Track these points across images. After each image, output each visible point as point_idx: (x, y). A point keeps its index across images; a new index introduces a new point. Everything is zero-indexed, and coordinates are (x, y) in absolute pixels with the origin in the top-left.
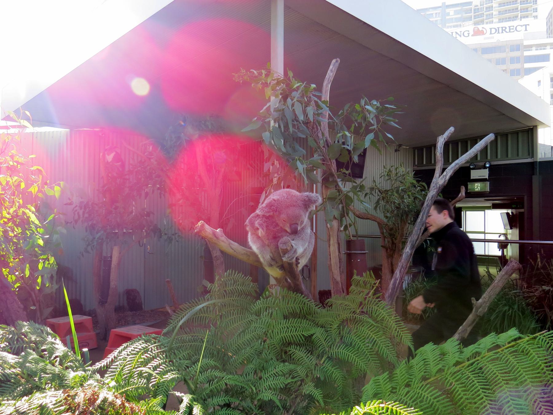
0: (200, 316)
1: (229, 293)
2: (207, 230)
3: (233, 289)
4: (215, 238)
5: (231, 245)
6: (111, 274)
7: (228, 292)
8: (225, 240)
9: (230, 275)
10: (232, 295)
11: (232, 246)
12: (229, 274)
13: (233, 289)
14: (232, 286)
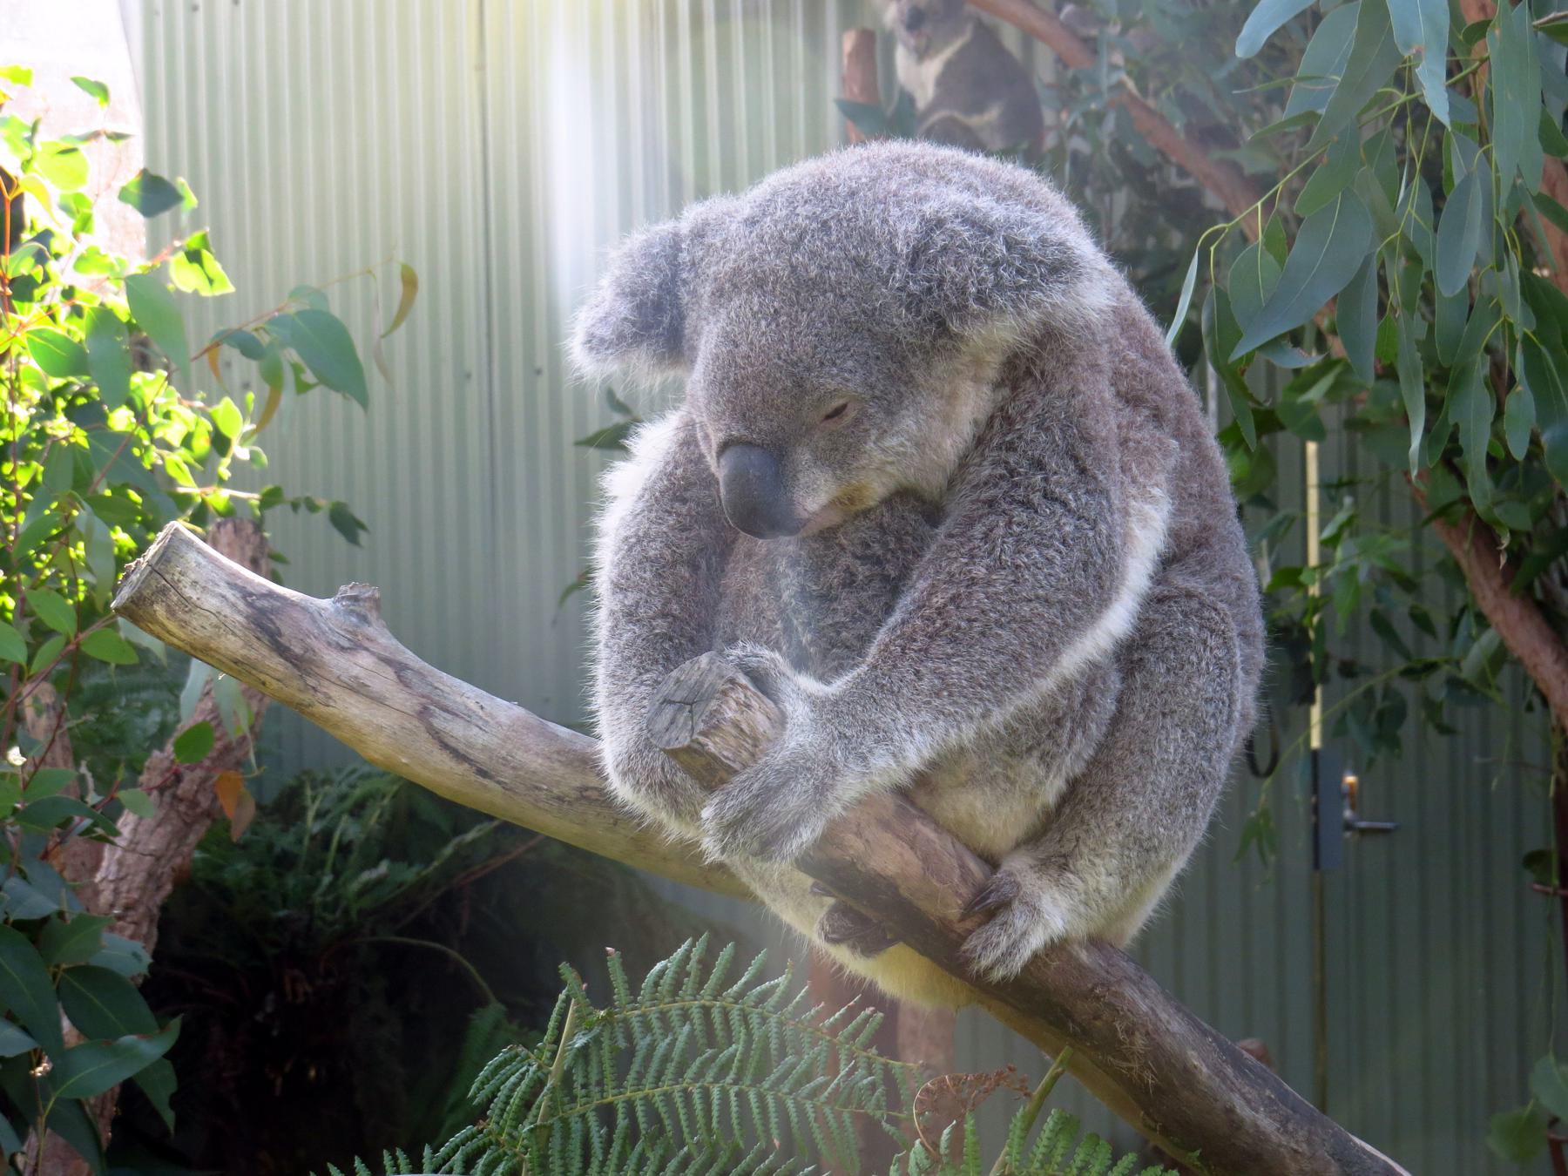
1: (633, 1135)
2: (189, 592)
3: (668, 1097)
4: (276, 663)
5: (441, 721)
7: (622, 1122)
8: (383, 681)
9: (689, 983)
11: (455, 730)
12: (681, 972)
14: (671, 1068)
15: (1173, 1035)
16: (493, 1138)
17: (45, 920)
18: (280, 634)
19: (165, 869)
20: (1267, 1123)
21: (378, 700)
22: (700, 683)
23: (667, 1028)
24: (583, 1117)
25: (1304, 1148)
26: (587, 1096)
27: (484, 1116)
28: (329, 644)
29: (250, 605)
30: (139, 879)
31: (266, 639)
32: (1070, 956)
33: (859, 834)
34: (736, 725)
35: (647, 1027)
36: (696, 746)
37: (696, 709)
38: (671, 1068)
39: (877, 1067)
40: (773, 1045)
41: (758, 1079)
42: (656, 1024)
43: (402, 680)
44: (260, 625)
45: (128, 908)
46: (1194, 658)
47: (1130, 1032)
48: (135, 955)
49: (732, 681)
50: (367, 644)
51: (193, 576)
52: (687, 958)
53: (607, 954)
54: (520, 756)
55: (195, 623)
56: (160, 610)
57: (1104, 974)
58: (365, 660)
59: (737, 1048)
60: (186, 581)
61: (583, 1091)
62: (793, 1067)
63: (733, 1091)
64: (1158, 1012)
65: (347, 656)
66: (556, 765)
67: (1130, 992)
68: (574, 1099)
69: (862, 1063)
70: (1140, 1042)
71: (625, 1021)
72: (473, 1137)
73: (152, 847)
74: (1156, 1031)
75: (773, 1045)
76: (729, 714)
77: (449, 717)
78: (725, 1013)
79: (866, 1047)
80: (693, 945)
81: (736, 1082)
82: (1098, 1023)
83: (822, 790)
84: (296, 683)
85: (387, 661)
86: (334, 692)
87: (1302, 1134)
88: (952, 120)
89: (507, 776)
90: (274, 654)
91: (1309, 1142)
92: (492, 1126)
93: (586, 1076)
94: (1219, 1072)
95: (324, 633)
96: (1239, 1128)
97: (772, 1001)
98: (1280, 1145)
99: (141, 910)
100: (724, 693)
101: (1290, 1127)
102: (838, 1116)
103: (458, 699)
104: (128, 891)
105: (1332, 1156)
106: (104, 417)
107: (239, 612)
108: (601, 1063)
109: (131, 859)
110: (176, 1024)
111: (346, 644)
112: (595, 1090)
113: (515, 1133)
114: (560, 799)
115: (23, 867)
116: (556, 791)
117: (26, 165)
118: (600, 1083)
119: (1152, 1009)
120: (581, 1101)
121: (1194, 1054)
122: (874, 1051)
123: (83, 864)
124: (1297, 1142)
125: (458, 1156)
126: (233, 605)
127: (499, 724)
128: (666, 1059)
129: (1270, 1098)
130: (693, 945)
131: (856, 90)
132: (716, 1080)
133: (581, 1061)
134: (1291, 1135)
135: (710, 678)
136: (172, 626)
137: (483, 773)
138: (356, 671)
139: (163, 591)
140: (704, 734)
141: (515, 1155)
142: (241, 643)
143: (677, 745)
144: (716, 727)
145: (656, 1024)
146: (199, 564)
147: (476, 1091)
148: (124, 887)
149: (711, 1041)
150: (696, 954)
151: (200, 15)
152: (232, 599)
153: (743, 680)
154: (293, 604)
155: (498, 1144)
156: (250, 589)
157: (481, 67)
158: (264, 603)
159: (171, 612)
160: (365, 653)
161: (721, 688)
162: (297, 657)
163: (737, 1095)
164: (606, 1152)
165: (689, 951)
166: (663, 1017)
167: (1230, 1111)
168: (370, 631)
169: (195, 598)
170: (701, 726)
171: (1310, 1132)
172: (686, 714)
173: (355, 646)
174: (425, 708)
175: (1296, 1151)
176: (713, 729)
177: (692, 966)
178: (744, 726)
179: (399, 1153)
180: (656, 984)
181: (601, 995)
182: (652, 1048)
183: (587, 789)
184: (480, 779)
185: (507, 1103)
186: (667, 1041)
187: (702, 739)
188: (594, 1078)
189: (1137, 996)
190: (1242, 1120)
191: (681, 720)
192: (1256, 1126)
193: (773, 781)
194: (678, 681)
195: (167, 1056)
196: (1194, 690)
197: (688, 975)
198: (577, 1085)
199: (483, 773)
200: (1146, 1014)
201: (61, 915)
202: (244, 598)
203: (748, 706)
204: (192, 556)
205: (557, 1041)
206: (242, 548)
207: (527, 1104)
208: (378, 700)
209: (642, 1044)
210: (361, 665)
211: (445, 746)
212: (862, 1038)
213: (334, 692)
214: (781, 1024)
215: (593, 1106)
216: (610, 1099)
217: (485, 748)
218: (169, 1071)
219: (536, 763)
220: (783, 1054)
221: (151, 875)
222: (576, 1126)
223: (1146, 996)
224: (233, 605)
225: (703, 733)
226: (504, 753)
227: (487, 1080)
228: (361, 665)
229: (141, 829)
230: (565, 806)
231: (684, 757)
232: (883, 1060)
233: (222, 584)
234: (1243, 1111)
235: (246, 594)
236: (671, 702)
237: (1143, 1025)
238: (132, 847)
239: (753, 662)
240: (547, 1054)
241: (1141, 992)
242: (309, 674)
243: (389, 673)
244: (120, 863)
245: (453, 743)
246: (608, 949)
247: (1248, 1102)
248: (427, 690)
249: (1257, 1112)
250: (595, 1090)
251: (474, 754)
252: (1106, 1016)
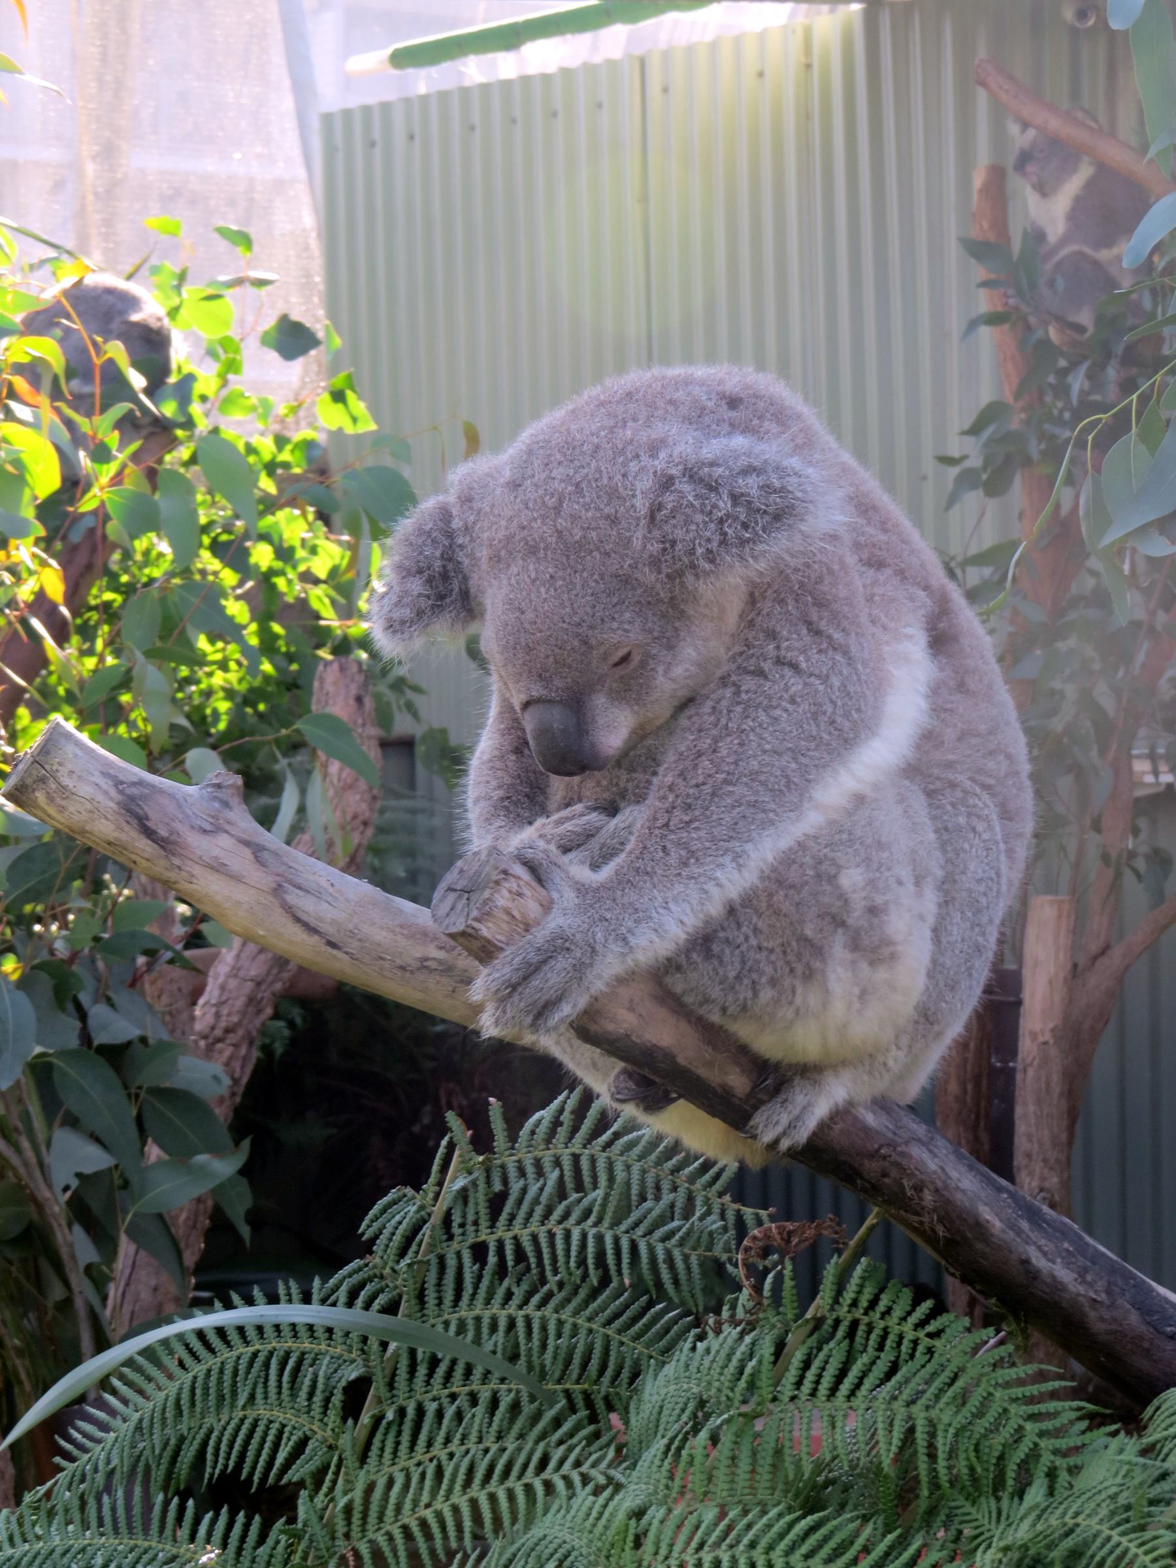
0: (251, 1414)
2: (66, 781)
3: (535, 1238)
4: (144, 845)
5: (294, 897)
6: (1019, 1110)
7: (492, 1259)
8: (241, 861)
9: (562, 1132)
10: (519, 1293)
11: (307, 905)
12: (556, 1123)
13: (535, 1238)
15: (964, 1192)
16: (377, 1271)
17: (129, 1044)
18: (148, 819)
19: (266, 994)
20: (1064, 1275)
21: (237, 878)
22: (478, 873)
23: (540, 1173)
24: (459, 1255)
25: (1103, 1297)
26: (463, 1234)
27: (371, 1253)
28: (192, 827)
29: (121, 792)
30: (240, 1003)
31: (135, 822)
32: (856, 1119)
33: (631, 1009)
34: (508, 912)
35: (522, 1172)
36: (470, 931)
37: (474, 897)
38: (539, 1211)
39: (731, 1216)
40: (635, 1190)
41: (616, 1223)
42: (530, 1170)
43: (258, 860)
44: (129, 811)
45: (228, 1031)
46: (967, 846)
47: (919, 1188)
48: (216, 1078)
49: (505, 872)
50: (227, 827)
51: (70, 766)
52: (561, 1111)
53: (488, 1104)
54: (367, 929)
55: (71, 809)
56: (40, 796)
57: (890, 1135)
58: (224, 841)
59: (599, 1193)
61: (460, 1231)
62: (650, 1210)
63: (592, 1233)
65: (208, 838)
66: (399, 938)
67: (918, 1152)
68: (451, 1237)
69: (716, 1209)
70: (928, 1197)
71: (503, 1167)
72: (360, 1269)
73: (253, 973)
74: (946, 1187)
75: (635, 1190)
77: (301, 893)
78: (593, 1161)
79: (720, 1195)
80: (568, 1097)
81: (596, 1225)
82: (887, 1180)
83: (579, 970)
84: (162, 863)
85: (246, 843)
86: (197, 870)
87: (1101, 1285)
88: (1081, 254)
89: (353, 946)
90: (142, 837)
91: (1109, 1292)
92: (377, 1260)
93: (464, 1216)
94: (1012, 1226)
95: (188, 817)
96: (1035, 1278)
97: (637, 1150)
98: (1079, 1294)
99: (241, 1032)
100: (497, 883)
101: (1089, 1278)
102: (686, 1258)
103: (311, 878)
104: (229, 1015)
105: (1133, 1305)
106: (246, 553)
107: (111, 799)
108: (477, 1204)
109: (233, 984)
110: (246, 1144)
111: (208, 827)
112: (470, 1229)
113: (397, 1268)
114: (403, 968)
115: (110, 993)
116: (399, 962)
117: (173, 312)
118: (476, 1223)
119: (942, 1169)
120: (457, 1239)
121: (986, 1209)
122: (727, 1198)
123: (180, 990)
124: (1096, 1292)
125: (344, 1288)
126: (106, 793)
127: (348, 900)
128: (536, 1201)
130: (568, 1097)
131: (985, 225)
132: (578, 1223)
133: (460, 1202)
134: (1091, 1285)
135: (487, 869)
136: (52, 811)
137: (332, 944)
138: (216, 852)
139: (43, 780)
140: (476, 919)
141: (396, 1287)
142: (112, 827)
143: (453, 930)
144: (488, 914)
145: (530, 1170)
146: (76, 755)
147: (366, 1228)
148: (225, 1011)
149: (579, 1187)
150: (571, 1104)
151: (378, 152)
152: (105, 787)
153: (519, 870)
154: (161, 791)
155: (382, 1277)
156: (122, 778)
157: (644, 199)
158: (134, 791)
159: (50, 799)
160: (225, 835)
161: (495, 878)
162: (163, 840)
163: (594, 1236)
164: (476, 1287)
165: (565, 1102)
166: (538, 1163)
167: (1026, 1262)
168: (230, 815)
169: (71, 786)
170: (475, 913)
171: (1109, 1283)
172: (464, 901)
173: (215, 829)
174: (280, 886)
175: (1095, 1300)
176: (486, 915)
177: (566, 1117)
178: (515, 913)
179: (292, 1283)
180: (533, 1133)
181: (482, 1142)
182: (524, 1191)
183: (427, 959)
184: (330, 950)
185: (390, 1240)
186: (539, 1185)
187: (475, 924)
188: (471, 1218)
189: (926, 1156)
190: (1038, 1271)
191: (459, 906)
192: (1053, 1277)
194: (461, 871)
195: (242, 1172)
197: (561, 1124)
198: (455, 1224)
199: (332, 944)
200: (935, 1172)
201: (143, 1040)
202: (116, 785)
203: (520, 895)
204: (70, 749)
205: (440, 1184)
206: (347, 686)
207: (409, 1240)
208: (237, 878)
209: (516, 1187)
210: (221, 846)
211: (298, 920)
212: (718, 1186)
213: (197, 870)
214: (644, 1172)
215: (468, 1244)
216: (483, 1237)
217: (333, 922)
218: (244, 1186)
219: (379, 935)
220: (643, 1199)
221: (251, 1000)
222: (451, 1262)
223: (935, 1156)
224: (106, 793)
225: (476, 919)
226: (351, 926)
227: (376, 1218)
228: (221, 846)
229: (243, 955)
230: (408, 975)
231: (462, 940)
232: (736, 1206)
233: (97, 773)
234: (1039, 1262)
235: (118, 783)
236: (455, 890)
237: (933, 1183)
238: (235, 972)
239: (529, 854)
240: (431, 1195)
241: (930, 1151)
242: (174, 855)
243: (247, 853)
244: (223, 988)
245: (305, 918)
246: (492, 1099)
247: (1045, 1254)
248: (281, 869)
249: (1054, 1262)
250: (470, 1229)
251: (324, 927)
252: (894, 1173)
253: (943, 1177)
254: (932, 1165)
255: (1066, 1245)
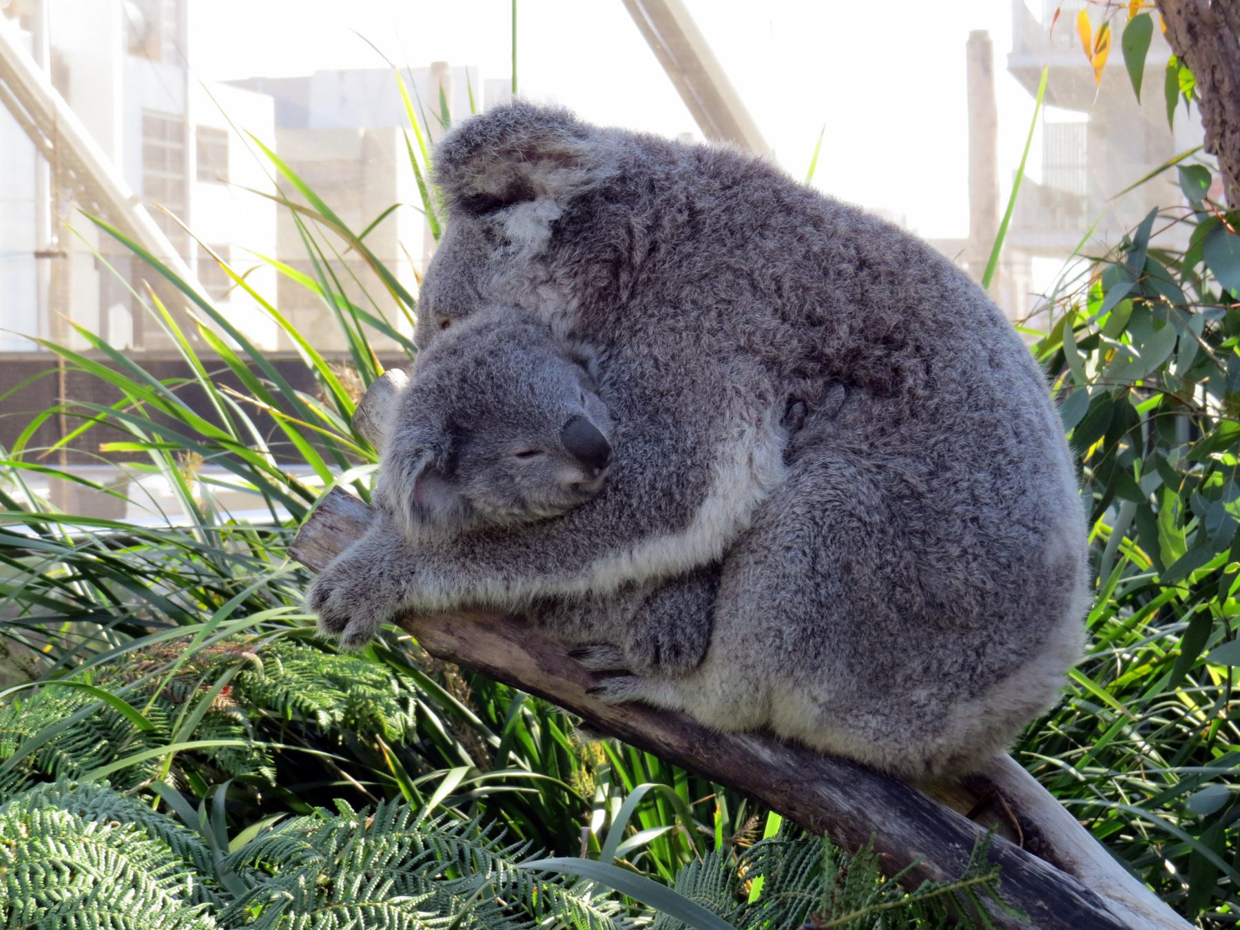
2: (375, 420)
15: (889, 835)
51: (378, 409)
57: (791, 773)
60: (373, 412)
64: (867, 812)
76: (311, 533)
119: (858, 810)
129: (1041, 908)
189: (838, 798)
193: (325, 586)
196: (771, 536)
200: (849, 813)
241: (845, 793)
253: (859, 818)
254: (845, 805)
255: (1040, 903)
